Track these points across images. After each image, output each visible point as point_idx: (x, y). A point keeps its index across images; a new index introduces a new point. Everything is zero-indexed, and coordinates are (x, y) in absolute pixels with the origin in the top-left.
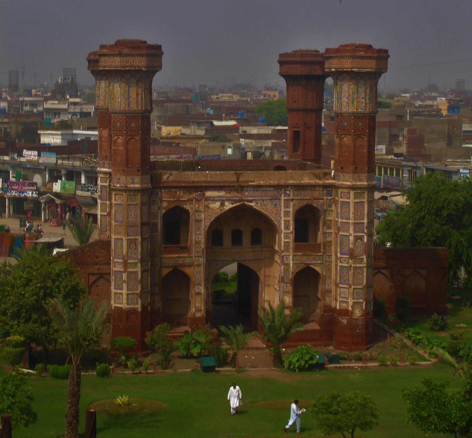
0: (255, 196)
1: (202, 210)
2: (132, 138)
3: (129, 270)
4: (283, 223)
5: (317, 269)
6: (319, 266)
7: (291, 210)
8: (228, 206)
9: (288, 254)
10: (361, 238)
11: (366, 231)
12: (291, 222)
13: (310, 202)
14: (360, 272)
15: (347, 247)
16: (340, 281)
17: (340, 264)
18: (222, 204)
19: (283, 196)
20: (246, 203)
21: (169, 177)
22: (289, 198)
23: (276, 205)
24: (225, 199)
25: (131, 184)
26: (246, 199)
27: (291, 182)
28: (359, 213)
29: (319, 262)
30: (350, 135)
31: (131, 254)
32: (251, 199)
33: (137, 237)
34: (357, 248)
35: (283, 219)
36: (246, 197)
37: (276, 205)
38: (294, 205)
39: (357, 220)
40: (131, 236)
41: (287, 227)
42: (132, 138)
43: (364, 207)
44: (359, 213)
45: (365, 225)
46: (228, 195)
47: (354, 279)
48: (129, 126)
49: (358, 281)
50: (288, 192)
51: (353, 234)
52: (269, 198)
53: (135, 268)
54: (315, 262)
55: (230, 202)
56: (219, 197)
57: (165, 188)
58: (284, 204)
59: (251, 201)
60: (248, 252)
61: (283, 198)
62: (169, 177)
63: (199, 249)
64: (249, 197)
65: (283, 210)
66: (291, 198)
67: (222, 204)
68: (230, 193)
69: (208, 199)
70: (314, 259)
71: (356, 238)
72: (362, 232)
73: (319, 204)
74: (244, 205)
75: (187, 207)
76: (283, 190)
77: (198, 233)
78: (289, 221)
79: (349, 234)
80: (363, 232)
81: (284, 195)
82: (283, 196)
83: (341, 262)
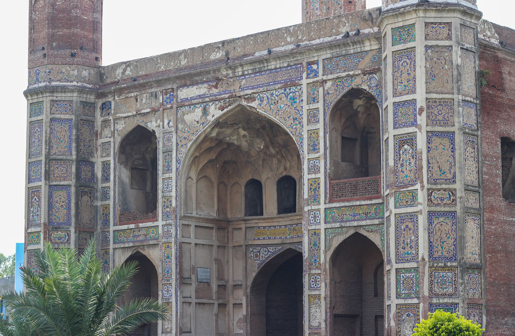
0: (258, 86)
1: (173, 129)
4: (305, 135)
5: (375, 238)
6: (376, 231)
7: (320, 105)
8: (215, 112)
9: (317, 207)
10: (411, 140)
11: (422, 119)
12: (321, 134)
13: (356, 83)
14: (410, 225)
18: (205, 112)
19: (304, 75)
20: (244, 103)
21: (125, 70)
22: (315, 79)
23: (294, 98)
24: (207, 99)
25: (35, 83)
26: (242, 94)
27: (317, 41)
28: (405, 76)
29: (376, 222)
31: (33, 216)
32: (250, 92)
33: (40, 183)
34: (402, 165)
35: (306, 128)
36: (243, 90)
37: (294, 98)
38: (326, 94)
39: (401, 95)
41: (314, 148)
44: (405, 76)
45: (421, 103)
46: (215, 91)
49: (408, 249)
50: (315, 67)
52: (279, 86)
54: (369, 222)
55: (218, 106)
56: (200, 96)
57: (120, 91)
58: (308, 94)
59: (250, 98)
61: (305, 82)
62: (125, 70)
63: (168, 209)
64: (248, 88)
65: (306, 107)
66: (320, 77)
67: (205, 112)
68: (216, 87)
69: (181, 105)
70: (366, 214)
73: (374, 83)
74: (240, 105)
75: (152, 126)
76: (305, 64)
77: (167, 175)
78: (316, 132)
80: (414, 123)
81: (308, 75)
82: (304, 75)
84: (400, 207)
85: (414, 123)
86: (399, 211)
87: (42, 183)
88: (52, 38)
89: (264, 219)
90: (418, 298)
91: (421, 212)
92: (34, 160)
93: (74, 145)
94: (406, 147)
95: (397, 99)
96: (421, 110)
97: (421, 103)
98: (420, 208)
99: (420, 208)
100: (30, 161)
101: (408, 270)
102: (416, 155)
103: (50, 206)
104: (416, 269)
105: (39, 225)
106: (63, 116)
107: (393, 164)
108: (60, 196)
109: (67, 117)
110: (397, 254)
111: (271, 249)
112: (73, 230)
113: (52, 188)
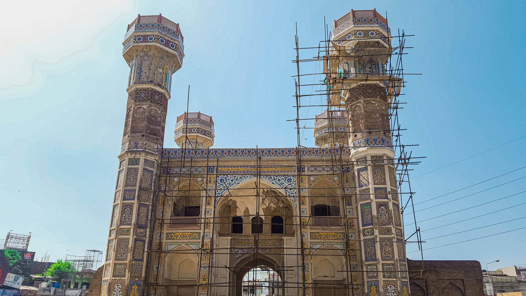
2: (140, 107)
3: (119, 237)
10: (386, 205)
14: (388, 243)
15: (370, 216)
16: (367, 260)
17: (365, 238)
30: (360, 102)
31: (125, 219)
33: (133, 201)
34: (381, 215)
39: (377, 184)
40: (128, 200)
42: (140, 107)
43: (384, 171)
47: (381, 252)
48: (139, 97)
51: (375, 200)
53: (127, 235)
60: (269, 240)
71: (379, 205)
72: (385, 198)
79: (369, 201)
80: (387, 197)
83: (364, 235)
84: (381, 234)
85: (387, 197)
86: (381, 236)
87: (135, 202)
88: (148, 128)
89: (242, 236)
90: (396, 278)
91: (394, 238)
92: (130, 188)
93: (153, 184)
94: (382, 207)
95: (377, 186)
96: (389, 192)
97: (389, 190)
98: (393, 236)
99: (393, 236)
100: (126, 188)
101: (388, 264)
102: (388, 211)
103: (138, 215)
104: (393, 264)
105: (130, 224)
106: (149, 168)
107: (376, 214)
108: (143, 210)
109: (152, 169)
110: (382, 257)
111: (245, 250)
112: (148, 230)
113: (140, 205)
